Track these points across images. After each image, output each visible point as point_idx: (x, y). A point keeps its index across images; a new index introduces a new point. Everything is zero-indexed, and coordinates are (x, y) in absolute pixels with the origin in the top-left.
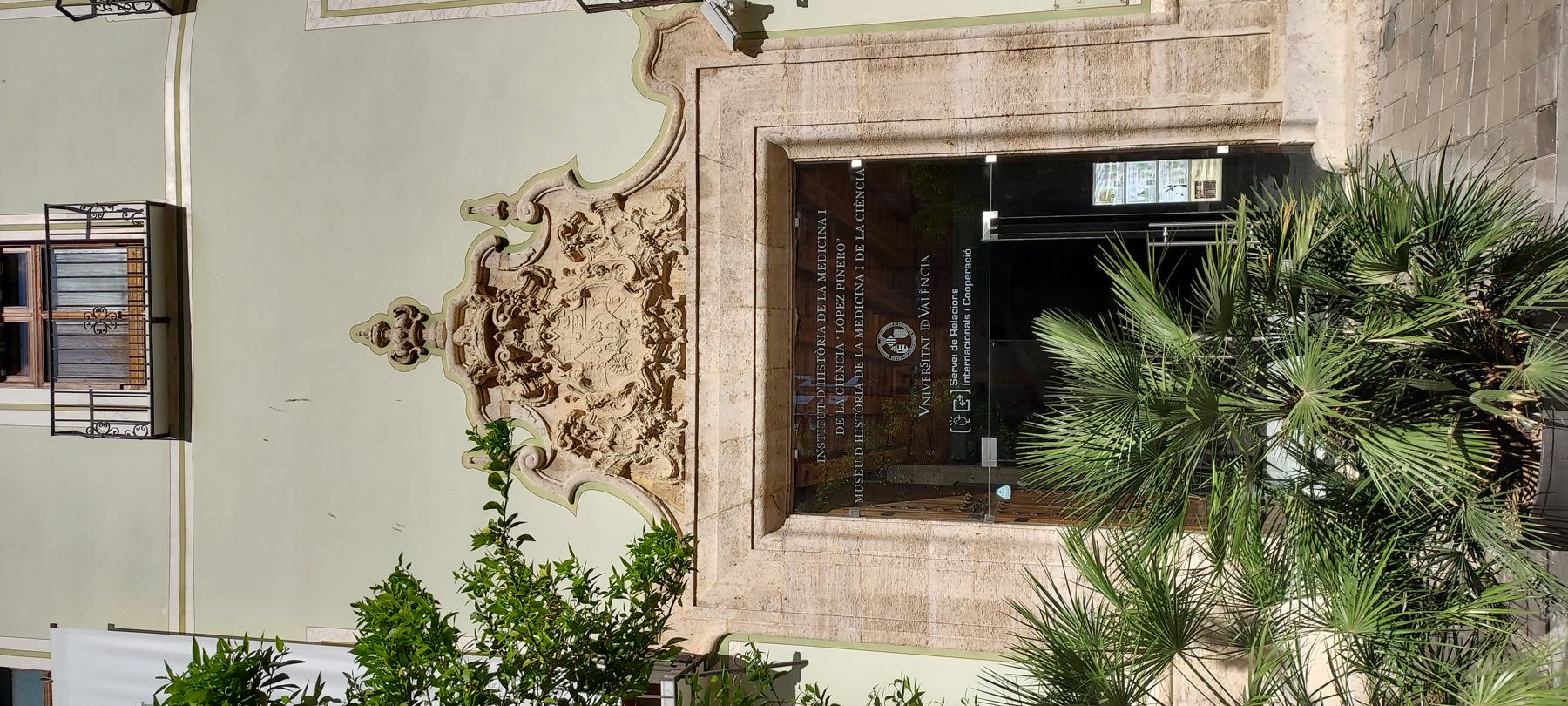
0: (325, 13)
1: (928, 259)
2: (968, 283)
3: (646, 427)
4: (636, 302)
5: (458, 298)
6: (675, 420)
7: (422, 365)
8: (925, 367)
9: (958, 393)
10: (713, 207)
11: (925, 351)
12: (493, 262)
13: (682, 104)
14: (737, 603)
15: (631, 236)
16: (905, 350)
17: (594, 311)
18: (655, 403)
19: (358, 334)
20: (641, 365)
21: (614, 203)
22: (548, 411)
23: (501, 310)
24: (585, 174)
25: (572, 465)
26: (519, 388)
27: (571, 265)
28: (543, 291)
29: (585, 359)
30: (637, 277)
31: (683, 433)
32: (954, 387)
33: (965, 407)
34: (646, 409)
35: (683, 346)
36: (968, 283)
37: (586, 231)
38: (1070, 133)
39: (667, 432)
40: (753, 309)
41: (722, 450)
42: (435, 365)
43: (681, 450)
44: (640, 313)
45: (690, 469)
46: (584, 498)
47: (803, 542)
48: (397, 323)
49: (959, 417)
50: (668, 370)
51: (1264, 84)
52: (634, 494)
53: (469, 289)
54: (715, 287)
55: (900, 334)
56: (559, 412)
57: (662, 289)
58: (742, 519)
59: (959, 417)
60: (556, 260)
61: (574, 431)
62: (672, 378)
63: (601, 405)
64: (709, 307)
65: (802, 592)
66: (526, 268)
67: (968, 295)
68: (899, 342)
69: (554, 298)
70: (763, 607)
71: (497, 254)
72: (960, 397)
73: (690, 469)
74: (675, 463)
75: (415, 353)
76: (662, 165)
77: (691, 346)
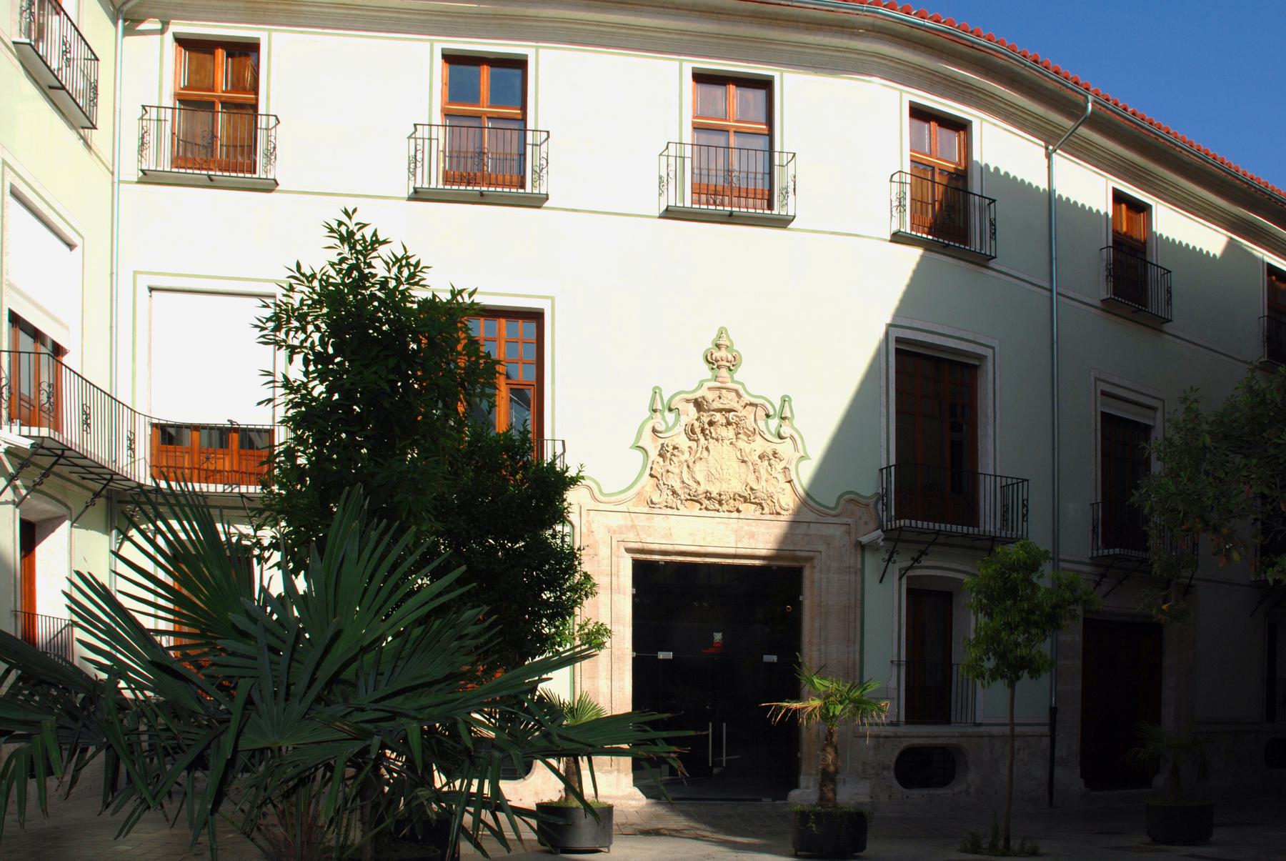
4: (738, 487)
7: (706, 367)
15: (772, 487)
17: (735, 464)
18: (689, 495)
19: (722, 332)
20: (710, 489)
21: (789, 479)
23: (736, 416)
27: (758, 452)
28: (745, 438)
29: (711, 459)
30: (752, 489)
34: (688, 491)
35: (718, 511)
39: (675, 500)
42: (706, 372)
44: (734, 490)
46: (639, 455)
48: (730, 358)
50: (706, 502)
56: (683, 442)
57: (746, 500)
58: (631, 536)
60: (758, 446)
61: (676, 452)
63: (688, 467)
74: (659, 503)
77: (717, 514)
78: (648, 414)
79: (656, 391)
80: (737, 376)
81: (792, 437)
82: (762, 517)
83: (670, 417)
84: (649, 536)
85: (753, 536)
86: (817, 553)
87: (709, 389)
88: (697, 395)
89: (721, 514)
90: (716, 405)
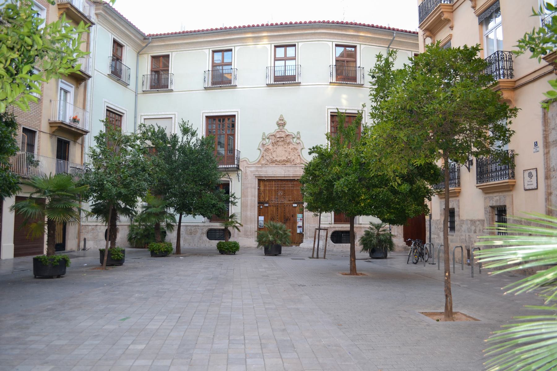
4: (285, 158)
5: (286, 132)
12: (291, 137)
14: (246, 172)
17: (284, 152)
19: (281, 116)
22: (271, 145)
24: (303, 150)
26: (273, 141)
27: (291, 148)
28: (287, 144)
37: (295, 150)
38: (305, 215)
42: (277, 127)
45: (263, 166)
46: (259, 151)
47: (254, 181)
48: (283, 122)
50: (276, 163)
51: (309, 237)
52: (260, 158)
53: (287, 133)
54: (287, 169)
56: (270, 147)
57: (287, 161)
58: (257, 173)
60: (291, 146)
64: (284, 168)
69: (286, 146)
73: (263, 166)
77: (279, 166)
78: (262, 140)
79: (264, 134)
80: (285, 128)
81: (299, 143)
83: (267, 140)
84: (261, 173)
87: (277, 132)
88: (274, 134)
89: (281, 166)
90: (278, 136)
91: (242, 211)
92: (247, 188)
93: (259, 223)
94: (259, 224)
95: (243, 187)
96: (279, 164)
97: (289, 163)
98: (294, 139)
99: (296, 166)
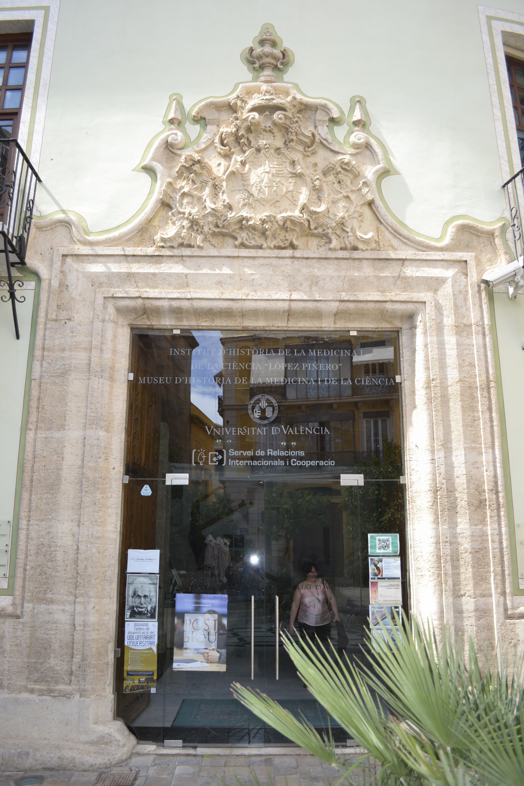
0: (489, 19)
1: (326, 432)
2: (308, 463)
3: (198, 218)
6: (205, 240)
8: (243, 430)
9: (223, 455)
10: (365, 271)
11: (256, 431)
13: (442, 249)
14: (63, 286)
16: (257, 414)
18: (217, 226)
19: (267, 28)
24: (386, 182)
25: (171, 168)
28: (301, 148)
31: (194, 247)
32: (228, 453)
33: (212, 461)
35: (260, 247)
36: (308, 463)
37: (347, 179)
40: (288, 298)
41: (180, 275)
43: (182, 245)
46: (146, 178)
48: (277, 52)
49: (204, 457)
50: (243, 236)
55: (269, 413)
59: (204, 457)
61: (196, 168)
62: (236, 239)
64: (288, 266)
65: (71, 334)
66: (317, 138)
67: (299, 463)
68: (263, 411)
70: (60, 306)
71: (327, 118)
72: (220, 457)
75: (254, 63)
76: (396, 233)
77: (260, 253)
82: (330, 255)
83: (194, 130)
85: (317, 283)
86: (418, 305)
91: (23, 514)
92: (64, 373)
93: (129, 591)
94: (130, 601)
95: (37, 365)
96: (260, 241)
97: (314, 242)
98: (336, 129)
99: (356, 254)
